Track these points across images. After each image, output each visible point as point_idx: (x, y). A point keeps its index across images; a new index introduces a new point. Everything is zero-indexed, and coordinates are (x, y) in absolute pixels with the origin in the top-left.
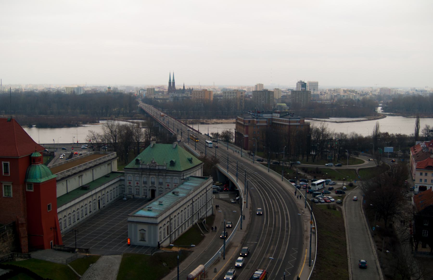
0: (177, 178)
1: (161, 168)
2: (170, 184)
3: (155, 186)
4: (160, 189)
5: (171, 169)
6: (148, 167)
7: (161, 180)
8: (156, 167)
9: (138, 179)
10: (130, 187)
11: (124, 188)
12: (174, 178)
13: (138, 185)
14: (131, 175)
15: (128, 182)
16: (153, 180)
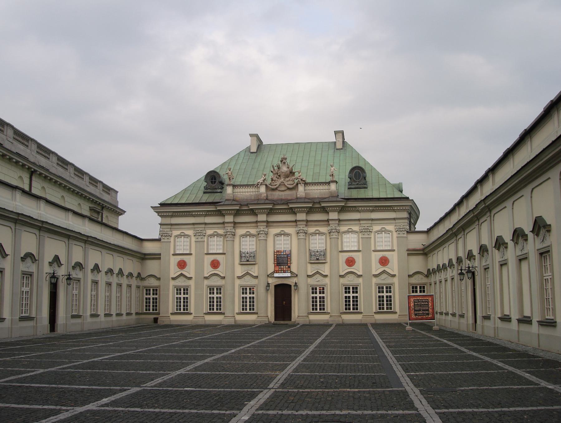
0: (391, 227)
1: (316, 191)
2: (358, 257)
5: (355, 194)
6: (263, 189)
7: (318, 243)
8: (295, 187)
9: (216, 245)
10: (181, 282)
11: (155, 291)
12: (376, 228)
13: (220, 271)
14: (190, 232)
15: (173, 261)
16: (283, 245)
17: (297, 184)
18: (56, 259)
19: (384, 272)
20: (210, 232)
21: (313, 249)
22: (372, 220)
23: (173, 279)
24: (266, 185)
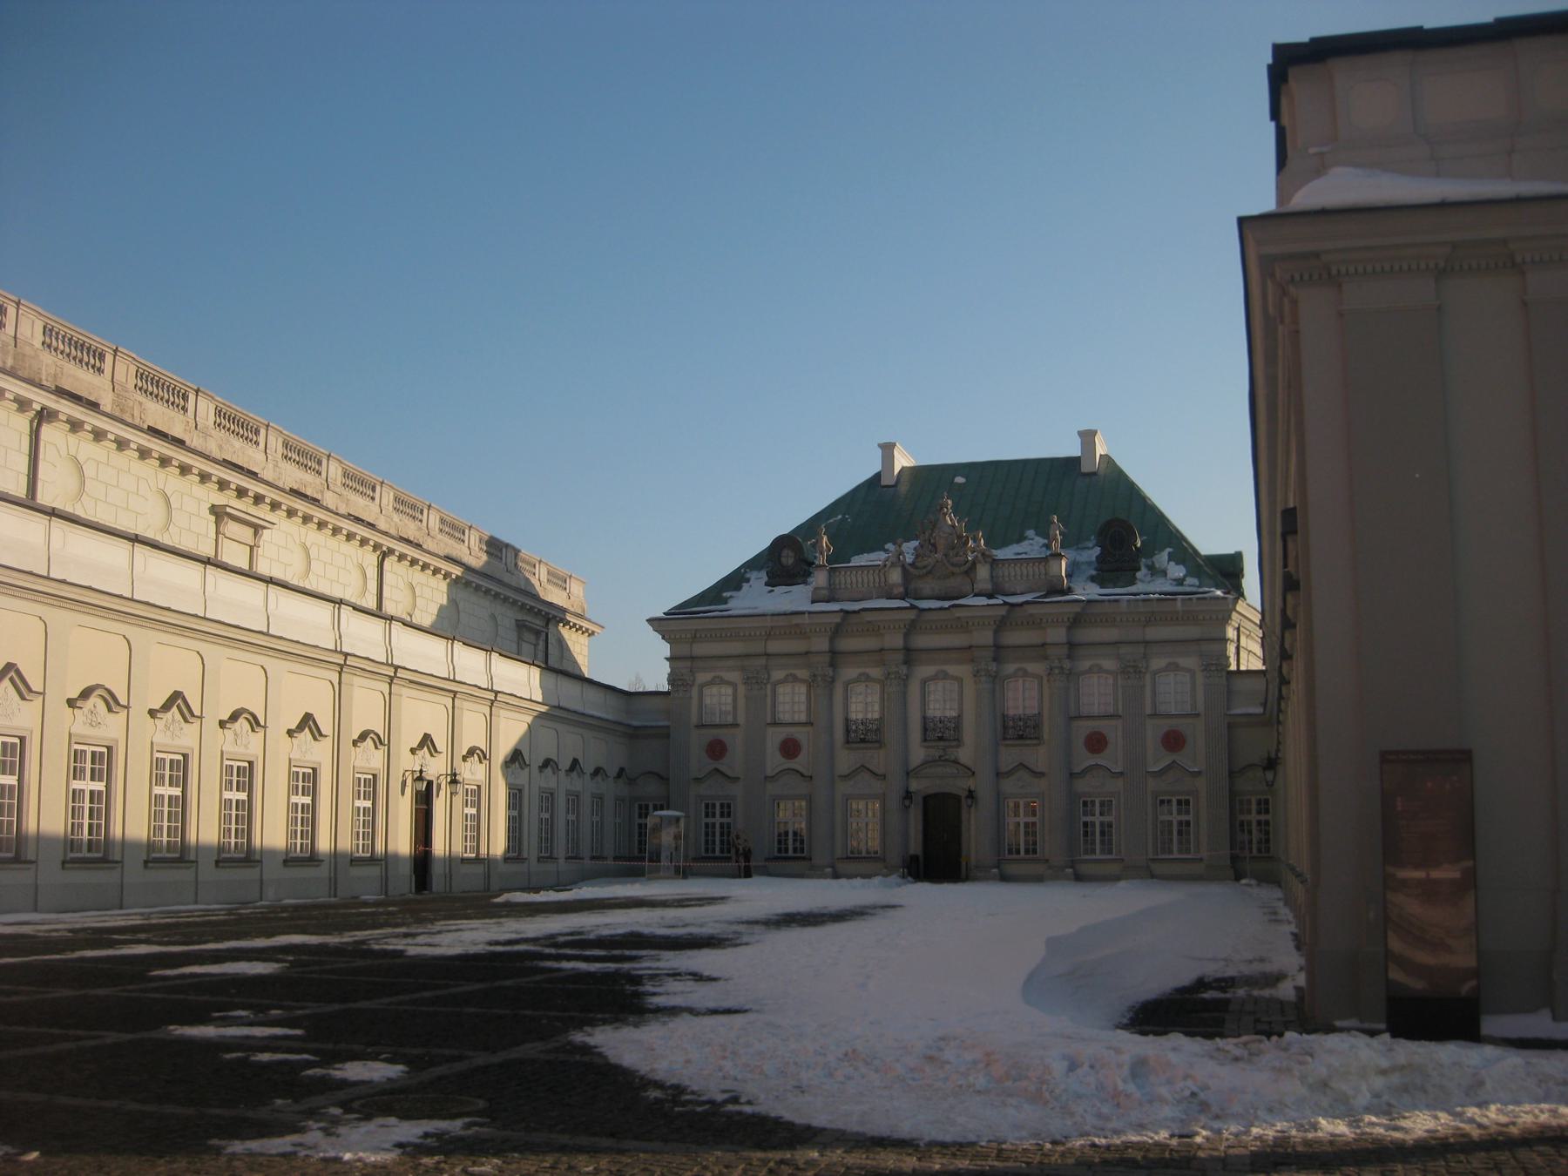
3: (965, 754)
4: (1008, 786)
7: (1022, 698)
13: (798, 763)
14: (734, 676)
16: (941, 704)
17: (974, 563)
18: (427, 741)
19: (1173, 765)
20: (778, 675)
21: (1011, 713)
22: (1146, 643)
23: (697, 779)
24: (903, 567)
